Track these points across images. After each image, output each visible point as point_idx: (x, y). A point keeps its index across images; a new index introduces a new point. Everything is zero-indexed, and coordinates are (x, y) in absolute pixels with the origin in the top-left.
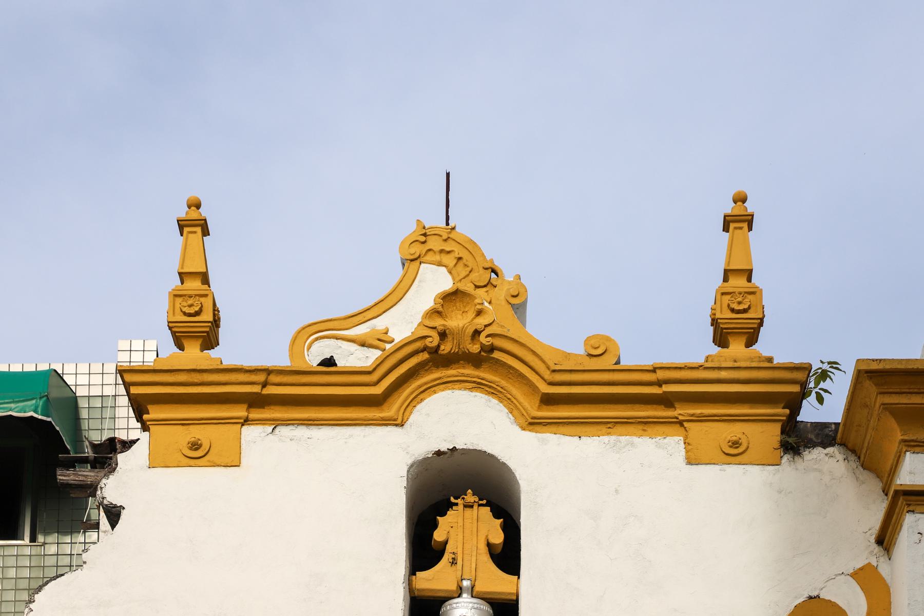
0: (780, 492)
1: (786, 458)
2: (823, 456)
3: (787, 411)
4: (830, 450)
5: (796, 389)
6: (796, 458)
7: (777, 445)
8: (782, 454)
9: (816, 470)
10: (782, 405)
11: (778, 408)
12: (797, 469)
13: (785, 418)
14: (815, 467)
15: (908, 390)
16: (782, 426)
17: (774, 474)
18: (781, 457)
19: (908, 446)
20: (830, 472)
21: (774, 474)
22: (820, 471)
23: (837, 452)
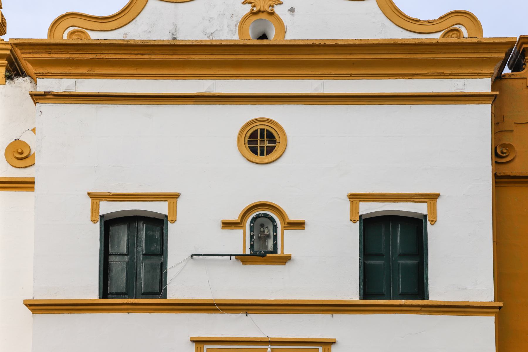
0: (5, 96)
1: (8, 81)
2: (22, 81)
3: (7, 62)
4: (26, 78)
5: (8, 52)
6: (12, 82)
7: (4, 76)
8: (6, 80)
9: (19, 87)
10: (5, 59)
11: (4, 61)
12: (12, 86)
13: (6, 65)
14: (20, 85)
15: (32, 52)
16: (6, 68)
17: (3, 89)
18: (6, 81)
19: (37, 75)
20: (25, 88)
21: (3, 89)
22: (21, 87)
23: (28, 79)
